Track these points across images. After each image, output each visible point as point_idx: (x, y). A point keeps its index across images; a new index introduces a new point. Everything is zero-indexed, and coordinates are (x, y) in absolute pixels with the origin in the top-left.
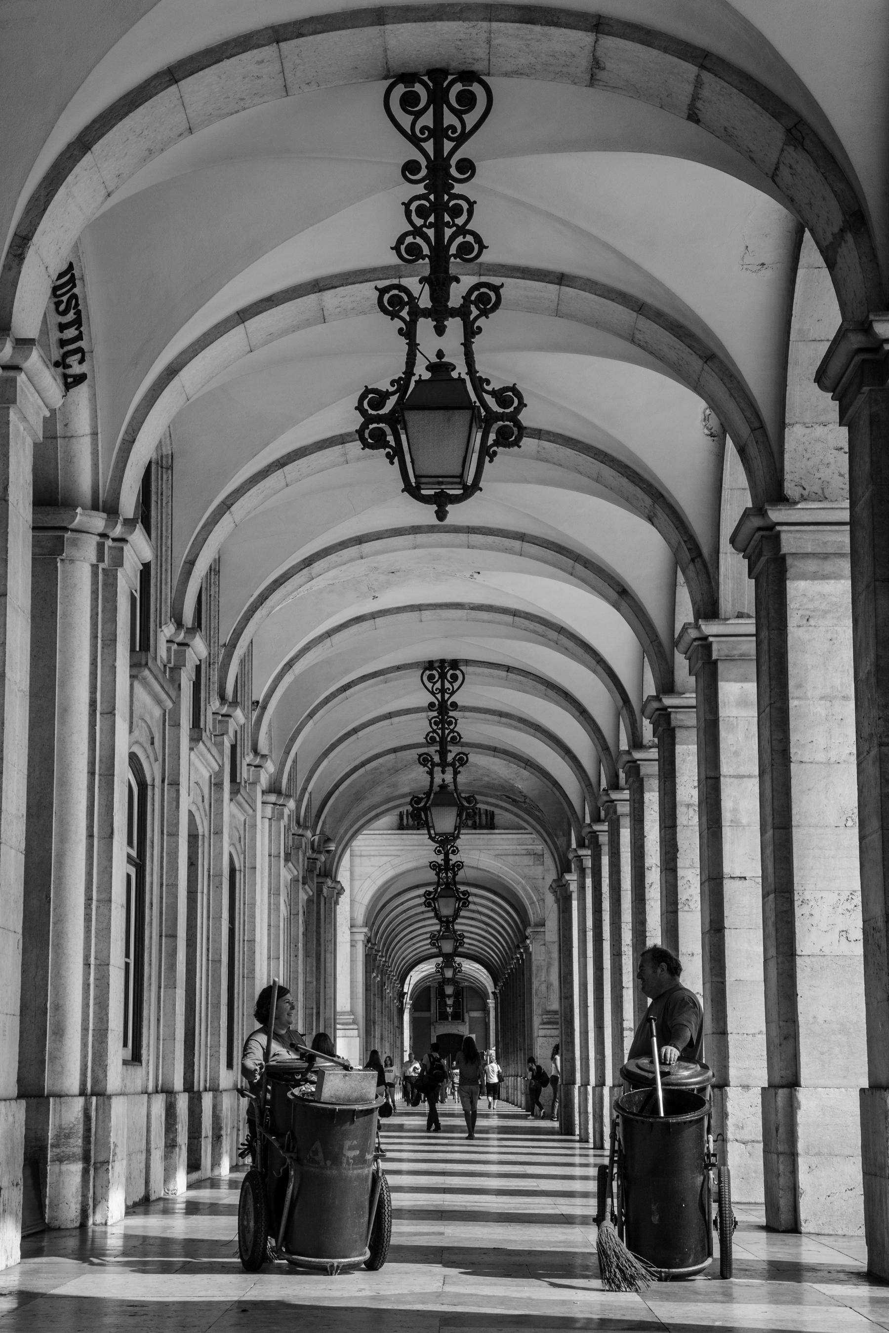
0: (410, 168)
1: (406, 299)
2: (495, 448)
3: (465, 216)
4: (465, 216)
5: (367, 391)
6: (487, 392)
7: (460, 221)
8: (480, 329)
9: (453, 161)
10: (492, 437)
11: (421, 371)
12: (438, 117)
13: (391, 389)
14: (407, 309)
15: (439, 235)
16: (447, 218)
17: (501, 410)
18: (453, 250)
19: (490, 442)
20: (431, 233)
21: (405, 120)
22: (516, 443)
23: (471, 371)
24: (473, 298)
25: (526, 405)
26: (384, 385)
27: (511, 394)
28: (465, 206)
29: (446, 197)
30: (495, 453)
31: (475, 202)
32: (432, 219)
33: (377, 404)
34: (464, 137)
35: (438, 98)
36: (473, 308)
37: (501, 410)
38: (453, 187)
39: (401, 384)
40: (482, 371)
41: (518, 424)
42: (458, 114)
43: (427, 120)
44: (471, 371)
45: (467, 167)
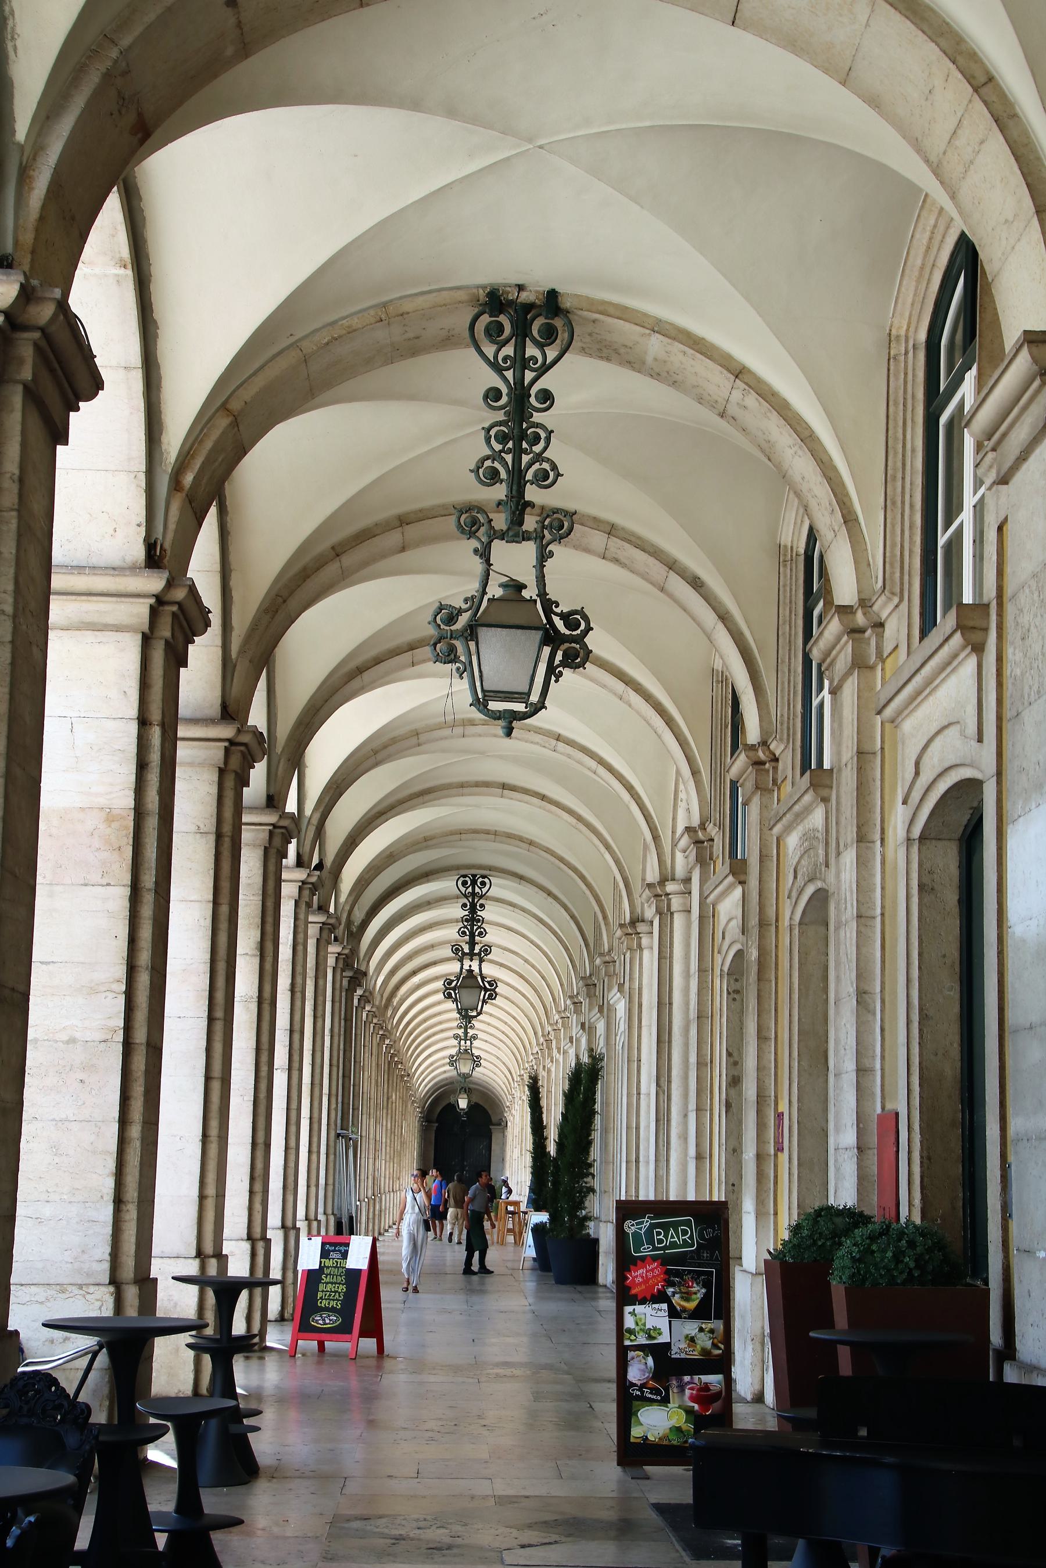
0: (493, 394)
1: (482, 521)
2: (561, 669)
3: (542, 444)
4: (542, 444)
5: (441, 608)
6: (556, 614)
7: (537, 449)
8: (551, 554)
9: (533, 391)
10: (559, 656)
11: (495, 590)
12: (520, 348)
13: (464, 606)
14: (483, 529)
15: (517, 460)
16: (525, 445)
17: (568, 632)
18: (529, 476)
19: (557, 662)
20: (509, 458)
21: (489, 350)
22: (582, 665)
23: (542, 594)
24: (546, 523)
25: (592, 629)
26: (459, 603)
27: (578, 617)
28: (543, 435)
29: (525, 425)
30: (561, 674)
31: (552, 431)
32: (510, 445)
33: (451, 619)
34: (545, 368)
35: (522, 332)
36: (546, 532)
37: (568, 632)
38: (532, 416)
39: (473, 602)
40: (552, 594)
41: (585, 646)
42: (541, 346)
43: (509, 350)
44: (542, 594)
45: (546, 396)
